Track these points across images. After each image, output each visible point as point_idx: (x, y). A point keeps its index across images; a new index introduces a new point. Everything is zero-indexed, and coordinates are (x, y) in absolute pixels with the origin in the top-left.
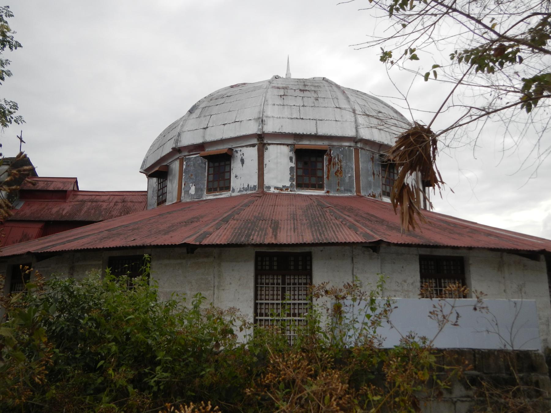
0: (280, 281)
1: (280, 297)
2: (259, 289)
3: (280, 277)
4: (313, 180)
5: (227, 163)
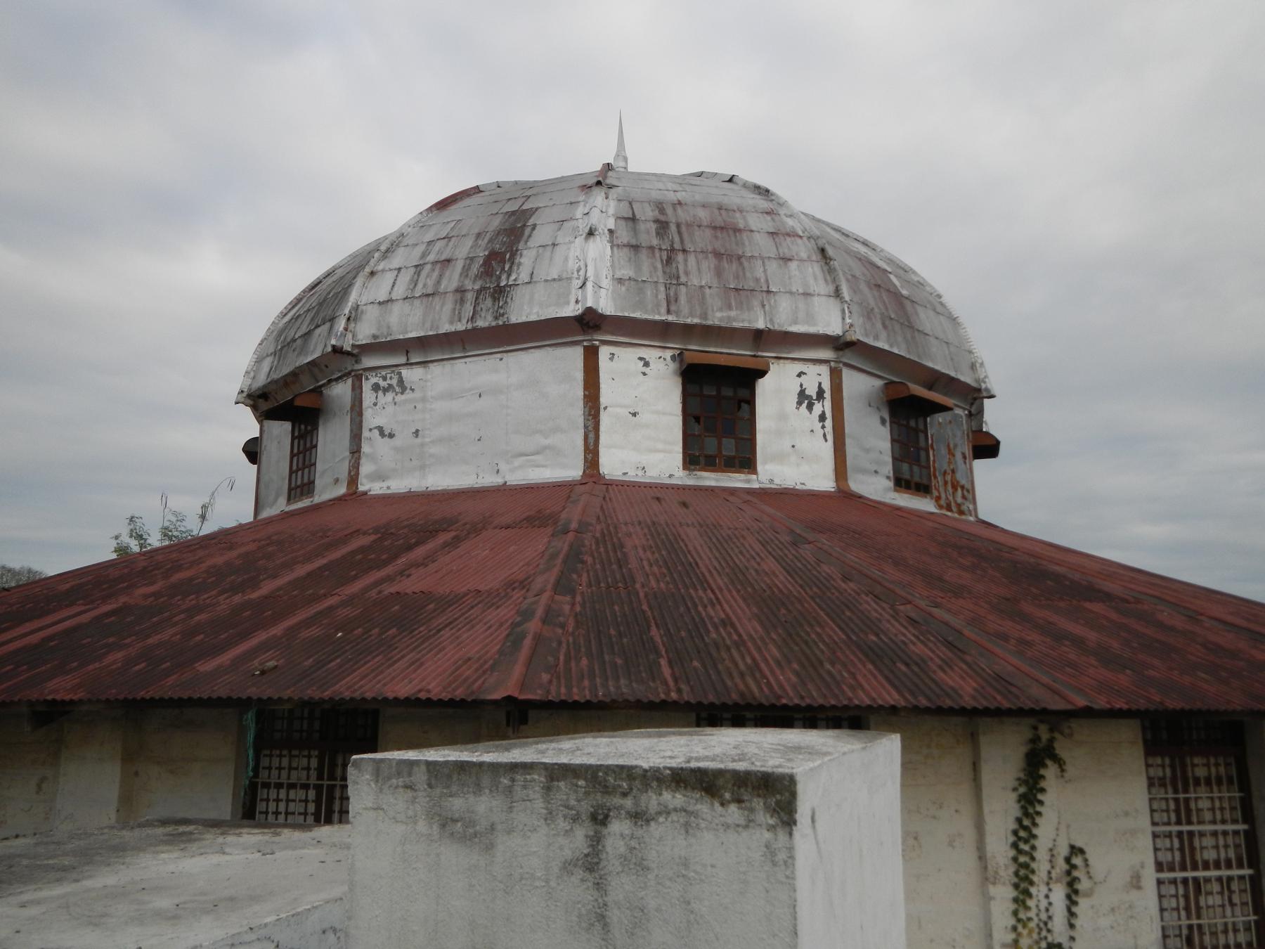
5: (743, 393)
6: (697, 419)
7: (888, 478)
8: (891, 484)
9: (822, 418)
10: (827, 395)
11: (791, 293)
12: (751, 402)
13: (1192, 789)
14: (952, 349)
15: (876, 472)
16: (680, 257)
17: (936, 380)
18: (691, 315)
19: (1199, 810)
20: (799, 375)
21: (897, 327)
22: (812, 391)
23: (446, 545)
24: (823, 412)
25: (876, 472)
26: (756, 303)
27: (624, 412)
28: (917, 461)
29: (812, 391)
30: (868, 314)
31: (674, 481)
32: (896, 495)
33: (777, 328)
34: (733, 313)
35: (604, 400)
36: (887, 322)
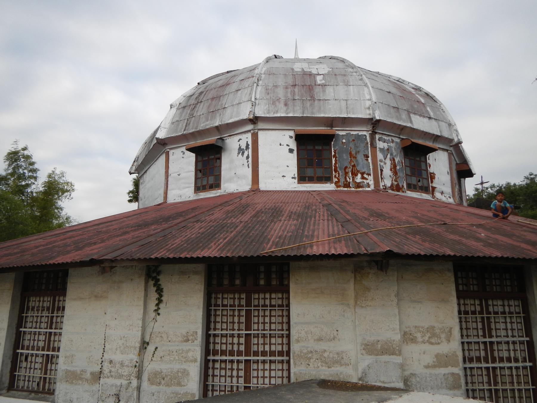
0: (243, 302)
1: (243, 326)
2: (213, 313)
3: (243, 296)
4: (320, 172)
5: (218, 156)
6: (200, 171)
7: (293, 178)
8: (296, 181)
9: (248, 157)
10: (250, 146)
11: (233, 105)
12: (220, 159)
13: (55, 312)
14: (349, 102)
15: (283, 176)
16: (199, 104)
17: (331, 122)
18: (192, 129)
19: (57, 322)
20: (239, 141)
21: (298, 103)
22: (244, 147)
23: (74, 237)
24: (248, 155)
25: (283, 176)
26: (218, 115)
27: (176, 175)
28: (320, 165)
29: (244, 147)
30: (274, 102)
31: (191, 199)
32: (299, 185)
33: (223, 123)
34: (208, 123)
35: (170, 172)
36: (290, 103)
